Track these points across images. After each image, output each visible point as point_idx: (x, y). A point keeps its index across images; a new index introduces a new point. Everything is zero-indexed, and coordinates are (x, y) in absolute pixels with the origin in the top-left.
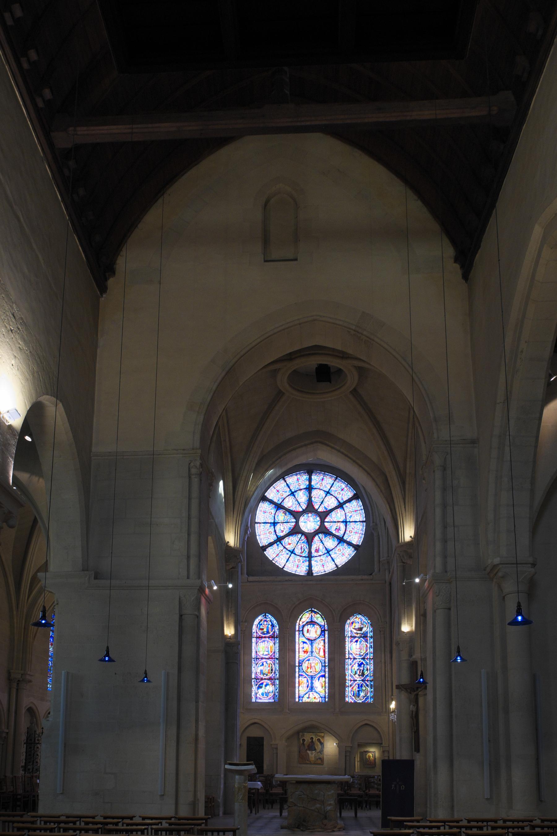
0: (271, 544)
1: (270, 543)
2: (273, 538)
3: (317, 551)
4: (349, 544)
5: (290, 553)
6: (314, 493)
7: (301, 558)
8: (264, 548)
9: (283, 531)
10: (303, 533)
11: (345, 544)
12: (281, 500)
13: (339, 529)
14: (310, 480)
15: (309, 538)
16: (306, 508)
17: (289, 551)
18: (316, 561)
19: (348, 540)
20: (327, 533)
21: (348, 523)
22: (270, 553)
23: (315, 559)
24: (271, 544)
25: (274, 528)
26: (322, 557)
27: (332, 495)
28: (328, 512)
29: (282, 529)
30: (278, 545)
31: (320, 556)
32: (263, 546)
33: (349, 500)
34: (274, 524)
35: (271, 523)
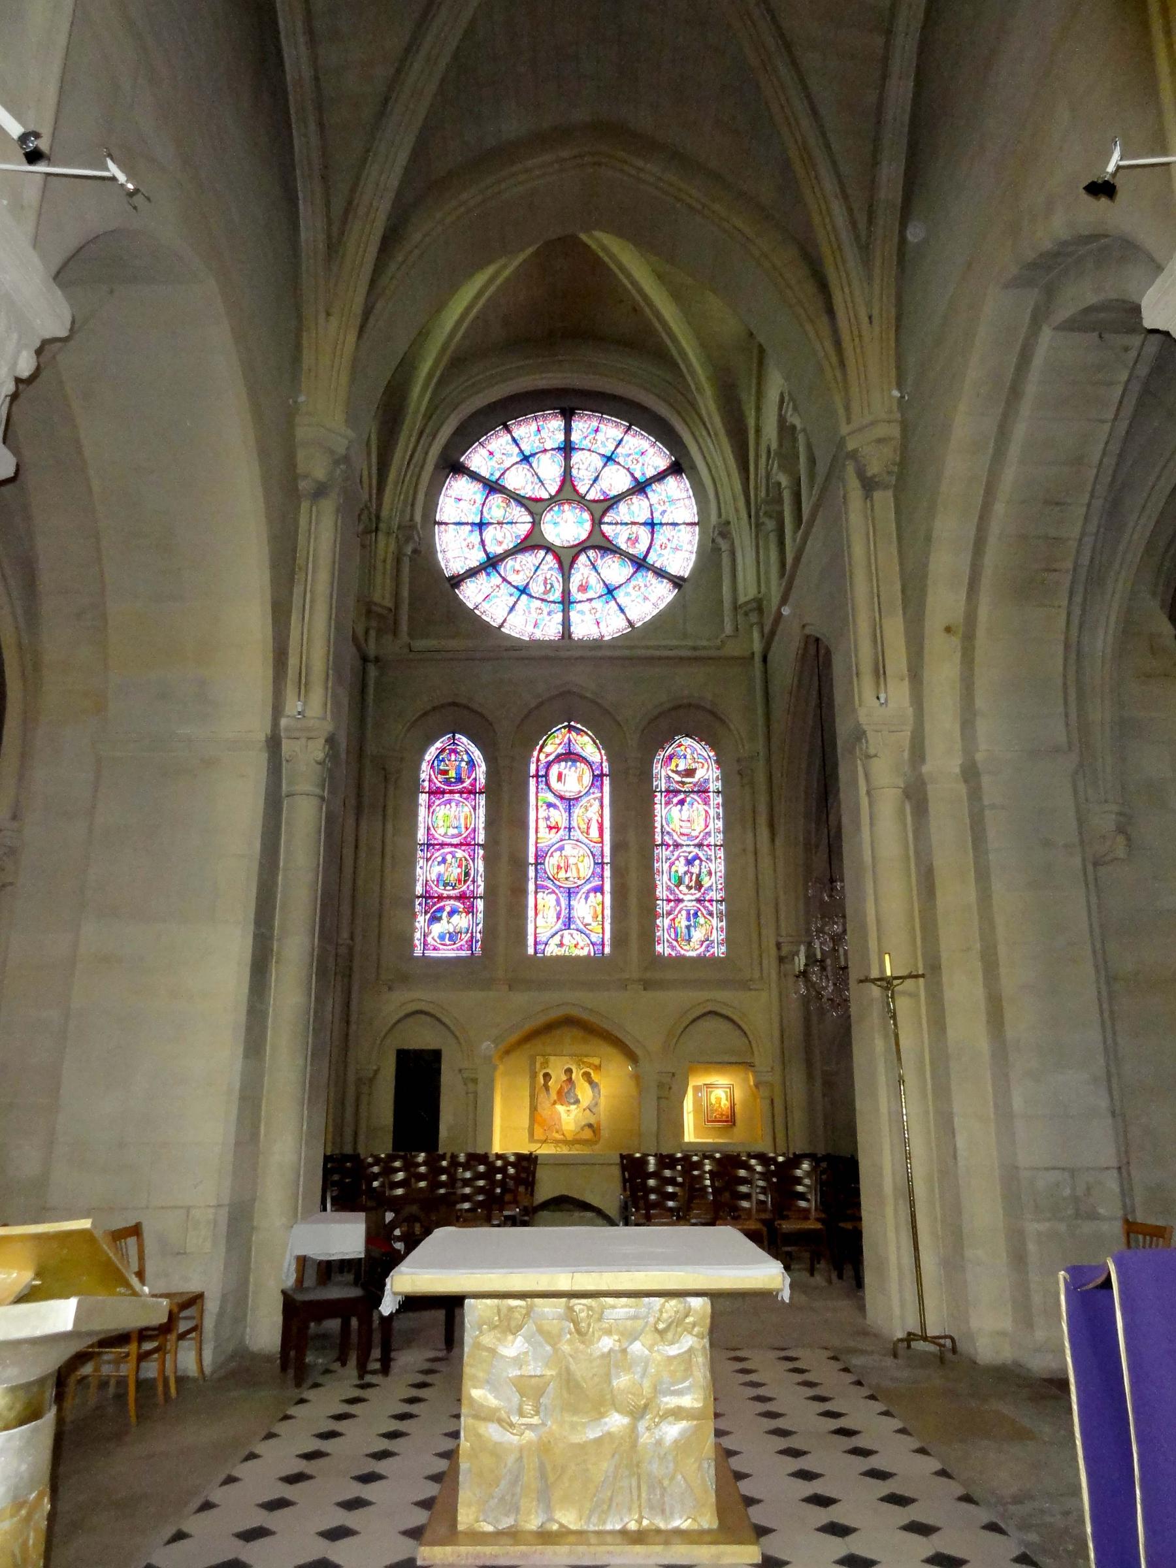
0: (472, 573)
1: (471, 569)
2: (476, 558)
3: (583, 588)
4: (660, 573)
5: (517, 593)
6: (576, 457)
7: (543, 605)
8: (456, 581)
9: (501, 543)
10: (549, 548)
11: (650, 574)
12: (497, 475)
13: (637, 540)
14: (568, 430)
15: (566, 559)
16: (558, 492)
17: (516, 588)
18: (582, 612)
19: (657, 565)
20: (607, 548)
21: (657, 528)
22: (471, 594)
23: (579, 607)
24: (472, 573)
25: (481, 534)
26: (595, 603)
27: (618, 463)
28: (611, 503)
29: (500, 539)
30: (488, 574)
31: (590, 600)
32: (453, 577)
33: (660, 477)
34: (481, 526)
35: (473, 524)
